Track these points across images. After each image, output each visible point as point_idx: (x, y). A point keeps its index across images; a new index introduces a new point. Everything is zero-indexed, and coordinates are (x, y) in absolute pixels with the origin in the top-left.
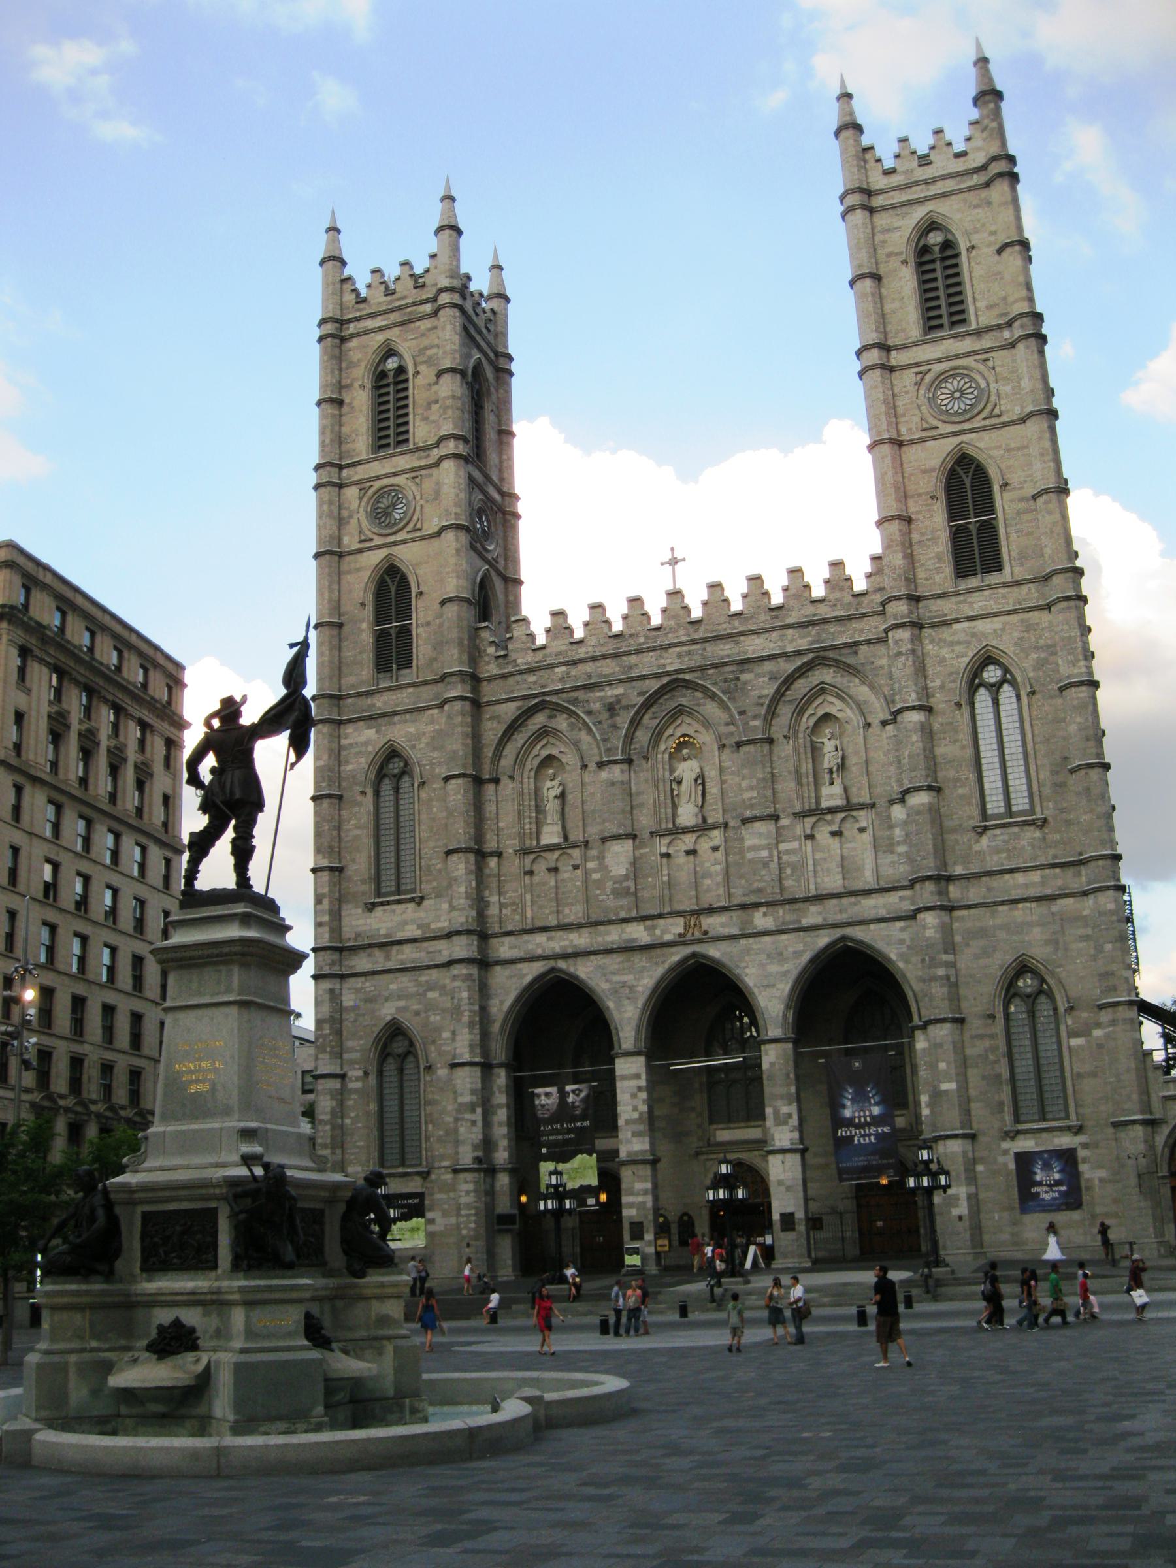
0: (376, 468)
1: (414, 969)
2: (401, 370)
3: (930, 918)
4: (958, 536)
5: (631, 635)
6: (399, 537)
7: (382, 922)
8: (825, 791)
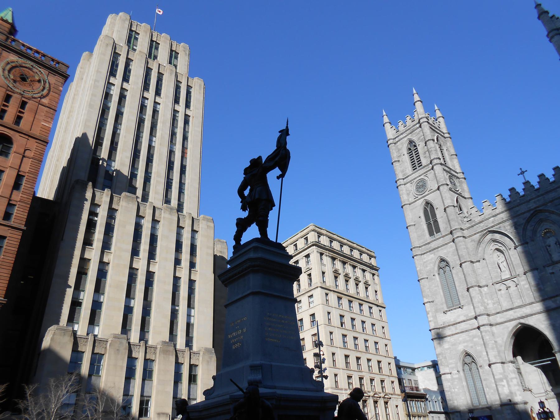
0: (414, 176)
1: (466, 331)
5: (514, 201)
6: (426, 193)
7: (452, 316)
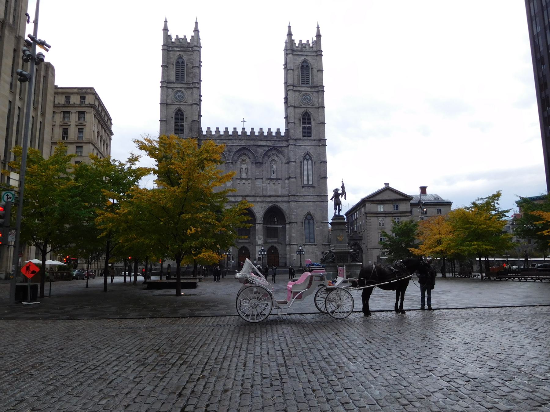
2: (183, 62)
3: (293, 203)
4: (304, 128)
8: (273, 175)
